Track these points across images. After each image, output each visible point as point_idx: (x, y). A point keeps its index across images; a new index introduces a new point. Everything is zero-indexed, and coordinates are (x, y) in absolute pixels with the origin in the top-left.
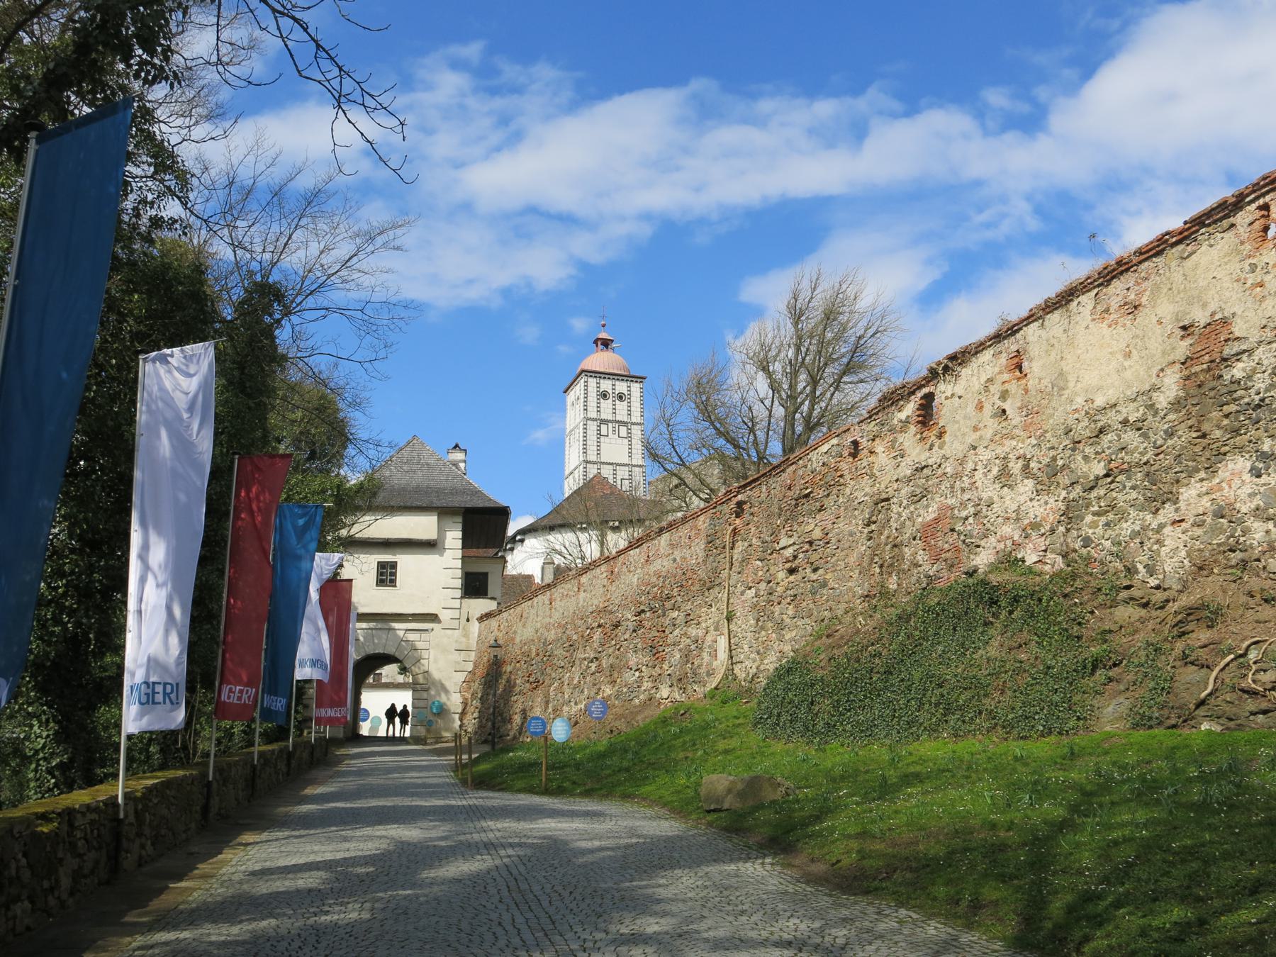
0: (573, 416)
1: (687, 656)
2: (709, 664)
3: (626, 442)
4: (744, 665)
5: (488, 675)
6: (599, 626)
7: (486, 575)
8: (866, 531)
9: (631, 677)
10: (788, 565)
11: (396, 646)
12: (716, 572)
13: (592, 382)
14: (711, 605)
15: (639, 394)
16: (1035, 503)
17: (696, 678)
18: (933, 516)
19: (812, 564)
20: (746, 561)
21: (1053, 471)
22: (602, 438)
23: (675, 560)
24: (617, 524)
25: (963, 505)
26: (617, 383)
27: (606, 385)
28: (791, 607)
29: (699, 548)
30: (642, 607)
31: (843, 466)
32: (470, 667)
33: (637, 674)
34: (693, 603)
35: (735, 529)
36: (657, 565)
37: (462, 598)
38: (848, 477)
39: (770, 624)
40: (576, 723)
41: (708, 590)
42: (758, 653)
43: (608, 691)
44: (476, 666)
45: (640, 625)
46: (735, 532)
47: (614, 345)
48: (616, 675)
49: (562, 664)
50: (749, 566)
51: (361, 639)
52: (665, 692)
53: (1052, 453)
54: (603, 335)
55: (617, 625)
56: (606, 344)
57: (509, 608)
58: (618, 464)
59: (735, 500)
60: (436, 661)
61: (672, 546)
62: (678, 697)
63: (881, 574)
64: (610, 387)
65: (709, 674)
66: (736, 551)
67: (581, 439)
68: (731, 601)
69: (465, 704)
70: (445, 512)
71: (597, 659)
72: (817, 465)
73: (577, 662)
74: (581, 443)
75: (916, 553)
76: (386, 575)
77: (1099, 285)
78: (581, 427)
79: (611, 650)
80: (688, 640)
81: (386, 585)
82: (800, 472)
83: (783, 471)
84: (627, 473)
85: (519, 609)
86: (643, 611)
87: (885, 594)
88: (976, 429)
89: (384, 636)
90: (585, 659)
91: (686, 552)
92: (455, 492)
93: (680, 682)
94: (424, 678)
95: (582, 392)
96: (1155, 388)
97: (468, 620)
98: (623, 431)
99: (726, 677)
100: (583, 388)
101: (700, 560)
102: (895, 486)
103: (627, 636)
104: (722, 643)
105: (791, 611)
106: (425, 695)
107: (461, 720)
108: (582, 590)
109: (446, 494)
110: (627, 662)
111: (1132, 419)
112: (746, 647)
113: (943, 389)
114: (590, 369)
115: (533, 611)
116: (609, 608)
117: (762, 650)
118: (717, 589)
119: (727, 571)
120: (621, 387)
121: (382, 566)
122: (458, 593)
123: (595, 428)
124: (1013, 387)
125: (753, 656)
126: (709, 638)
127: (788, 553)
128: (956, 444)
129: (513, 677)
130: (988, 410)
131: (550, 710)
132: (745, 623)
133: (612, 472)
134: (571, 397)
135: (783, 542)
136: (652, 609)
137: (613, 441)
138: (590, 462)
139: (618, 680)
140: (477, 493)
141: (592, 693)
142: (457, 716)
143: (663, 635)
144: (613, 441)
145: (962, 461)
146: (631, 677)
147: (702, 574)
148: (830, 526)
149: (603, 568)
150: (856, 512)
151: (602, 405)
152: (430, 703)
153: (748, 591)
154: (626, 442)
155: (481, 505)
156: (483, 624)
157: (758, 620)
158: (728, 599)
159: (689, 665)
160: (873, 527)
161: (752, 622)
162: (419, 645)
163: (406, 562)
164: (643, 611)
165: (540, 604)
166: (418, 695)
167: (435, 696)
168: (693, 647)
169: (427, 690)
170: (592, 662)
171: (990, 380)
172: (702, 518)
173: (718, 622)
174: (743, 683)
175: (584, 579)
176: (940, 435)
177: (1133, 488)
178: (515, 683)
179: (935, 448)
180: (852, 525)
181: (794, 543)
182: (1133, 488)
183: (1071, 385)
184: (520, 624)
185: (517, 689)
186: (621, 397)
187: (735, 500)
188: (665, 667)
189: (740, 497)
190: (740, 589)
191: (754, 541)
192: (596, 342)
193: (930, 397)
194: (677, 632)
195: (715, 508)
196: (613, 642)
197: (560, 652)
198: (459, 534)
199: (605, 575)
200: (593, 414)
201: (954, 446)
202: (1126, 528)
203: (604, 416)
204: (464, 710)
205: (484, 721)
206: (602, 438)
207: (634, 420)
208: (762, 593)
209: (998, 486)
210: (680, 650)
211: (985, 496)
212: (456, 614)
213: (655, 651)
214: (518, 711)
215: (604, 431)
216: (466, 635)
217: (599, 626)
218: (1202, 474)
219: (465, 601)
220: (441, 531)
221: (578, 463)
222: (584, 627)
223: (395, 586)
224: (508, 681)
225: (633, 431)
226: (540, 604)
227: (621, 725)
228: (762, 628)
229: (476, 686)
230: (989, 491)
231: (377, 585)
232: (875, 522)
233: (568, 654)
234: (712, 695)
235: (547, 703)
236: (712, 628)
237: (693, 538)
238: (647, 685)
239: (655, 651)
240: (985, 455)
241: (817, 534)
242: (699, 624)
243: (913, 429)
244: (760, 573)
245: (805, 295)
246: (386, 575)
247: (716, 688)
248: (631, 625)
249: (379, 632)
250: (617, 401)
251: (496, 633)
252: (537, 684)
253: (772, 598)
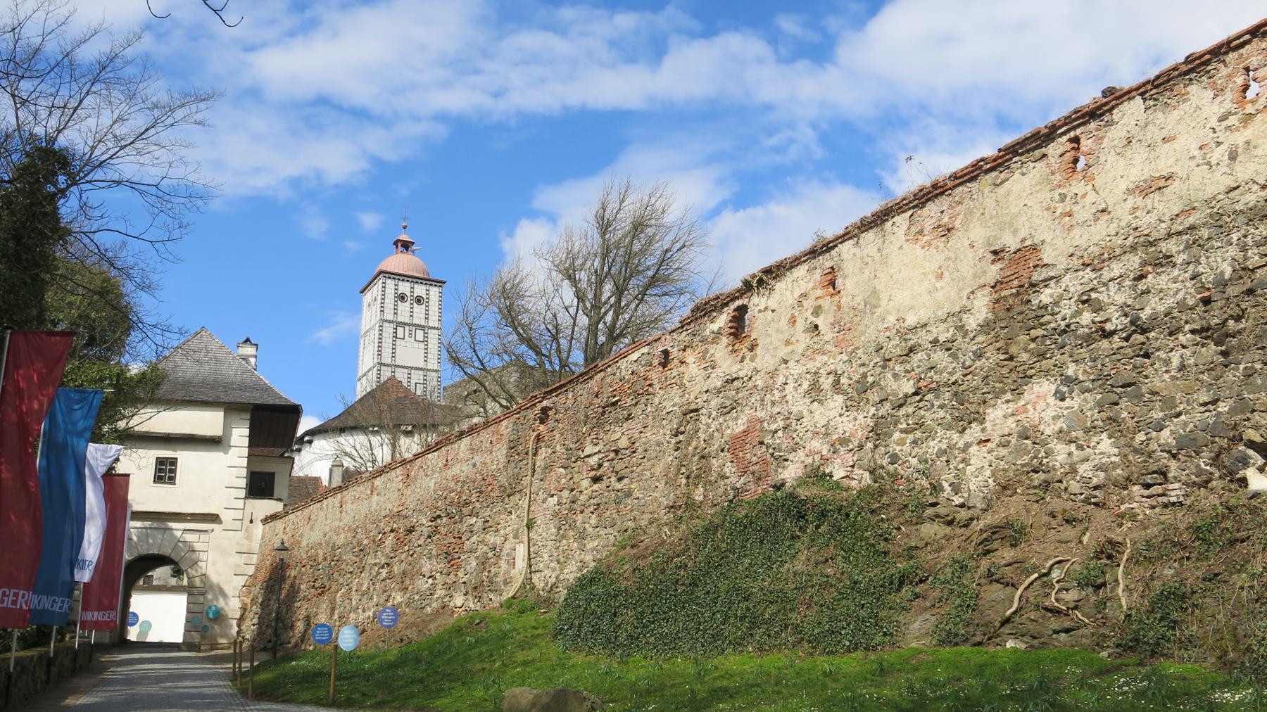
0: (369, 317)
1: (483, 564)
2: (507, 572)
3: (422, 346)
4: (543, 574)
5: (270, 579)
6: (392, 531)
7: (272, 475)
8: (673, 441)
9: (423, 584)
10: (592, 474)
11: (172, 547)
12: (518, 478)
13: (390, 284)
14: (511, 512)
15: (437, 299)
16: (844, 419)
17: (493, 587)
18: (742, 428)
19: (617, 473)
20: (548, 468)
21: (863, 387)
22: (398, 341)
23: (474, 465)
24: (410, 428)
25: (773, 418)
26: (416, 286)
27: (405, 287)
28: (594, 516)
29: (501, 453)
30: (438, 513)
31: (653, 375)
32: (251, 570)
33: (430, 581)
34: (492, 509)
35: (539, 435)
36: (455, 470)
37: (246, 498)
38: (657, 386)
39: (571, 533)
40: (363, 631)
41: (509, 496)
42: (558, 562)
43: (398, 598)
44: (257, 570)
45: (435, 531)
46: (539, 438)
47: (414, 248)
48: (407, 582)
49: (351, 570)
50: (552, 473)
51: (135, 538)
52: (459, 600)
53: (863, 370)
54: (404, 237)
55: (410, 531)
56: (406, 246)
57: (296, 510)
58: (412, 368)
59: (539, 406)
60: (214, 564)
61: (473, 450)
62: (472, 606)
63: (687, 485)
64: (409, 289)
65: (506, 583)
66: (539, 458)
67: (377, 341)
68: (532, 508)
69: (244, 609)
70: (232, 408)
71: (388, 565)
72: (626, 374)
73: (367, 568)
74: (376, 345)
75: (724, 465)
76: (165, 472)
77: (914, 207)
78: (377, 329)
79: (403, 556)
80: (486, 548)
81: (165, 483)
82: (608, 380)
83: (591, 378)
84: (422, 378)
85: (307, 511)
86: (439, 516)
87: (691, 505)
88: (788, 343)
89: (160, 536)
90: (375, 564)
91: (488, 459)
92: (244, 387)
93: (476, 590)
94: (202, 581)
95: (380, 293)
96: (965, 310)
97: (251, 522)
98: (420, 334)
99: (523, 585)
100: (380, 286)
101: (501, 466)
102: (705, 397)
103: (421, 542)
104: (521, 551)
105: (594, 521)
106: (201, 599)
107: (239, 626)
108: (375, 493)
109: (234, 389)
110: (420, 568)
111: (941, 339)
112: (546, 556)
113: (756, 302)
114: (389, 270)
115: (322, 514)
116: (403, 513)
117: (562, 560)
118: (518, 496)
119: (528, 478)
120: (420, 290)
121: (161, 462)
122: (242, 493)
124: (826, 303)
125: (553, 565)
126: (508, 546)
127: (593, 461)
128: (768, 357)
129: (297, 582)
130: (801, 325)
131: (336, 617)
132: (545, 531)
133: (406, 376)
134: (368, 297)
135: (589, 449)
136: (448, 514)
137: (408, 344)
138: (384, 365)
139: (410, 587)
140: (267, 389)
141: (382, 601)
142: (234, 622)
143: (459, 542)
144: (408, 344)
145: (773, 375)
146: (423, 584)
147: (503, 480)
148: (637, 435)
149: (399, 471)
150: (664, 422)
151: (399, 308)
152: (206, 607)
153: (549, 499)
154: (422, 346)
155: (271, 402)
156: (267, 526)
157: (559, 529)
158: (529, 507)
159: (487, 574)
160: (681, 437)
161: (554, 530)
162: (197, 546)
163: (187, 459)
164: (439, 516)
165: (330, 507)
166: (193, 599)
167: (212, 601)
168: (490, 555)
169: (203, 594)
170: (383, 567)
171: (804, 295)
172: (505, 423)
173: (518, 530)
174: (541, 593)
175: (378, 482)
176: (752, 348)
177: (941, 407)
178: (299, 588)
179: (747, 361)
180: (660, 434)
181: (600, 452)
182: (941, 407)
183: (883, 303)
184: (308, 527)
185: (301, 595)
186: (419, 300)
187: (539, 406)
188: (461, 574)
189: (545, 403)
190: (541, 496)
191: (558, 447)
192: (396, 243)
193: (743, 310)
194: (474, 539)
195: (518, 413)
196: (407, 548)
197: (349, 557)
198: (246, 432)
199: (400, 478)
200: (390, 317)
201: (765, 359)
202: (933, 446)
203: (400, 319)
204: (242, 615)
205: (264, 628)
206: (398, 341)
207: (431, 324)
208: (564, 501)
209: (808, 401)
210: (477, 558)
211: (795, 409)
212: (239, 515)
213: (450, 558)
214: (301, 617)
215: (400, 334)
216: (249, 538)
217: (392, 531)
218: (1008, 396)
219: (247, 501)
220: (227, 427)
221: (372, 365)
222: (377, 532)
223: (174, 484)
224: (292, 586)
225: (430, 336)
226: (330, 507)
227: (412, 634)
228: (563, 537)
229: (257, 590)
230: (799, 405)
231: (154, 482)
232: (682, 433)
233: (357, 559)
234: (509, 604)
235: (333, 609)
236: (511, 536)
237: (494, 443)
238: (440, 593)
239: (450, 558)
240: (796, 369)
241: (623, 443)
242: (497, 531)
243: (725, 340)
244: (564, 481)
245: (613, 205)
246: (165, 472)
247: (513, 597)
248: (426, 531)
249: (155, 532)
250: (415, 304)
251: (281, 535)
252: (323, 590)
253: (575, 506)
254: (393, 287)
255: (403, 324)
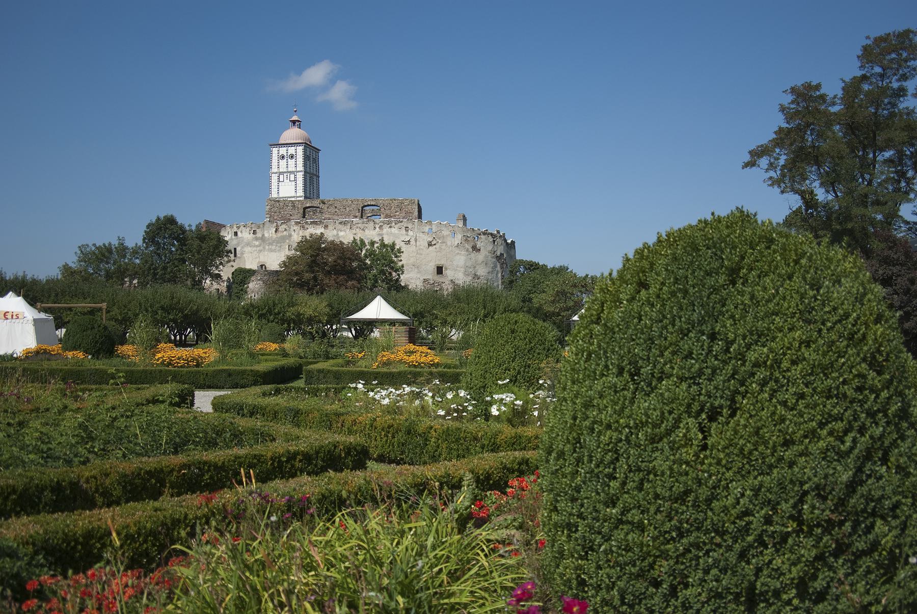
13: (275, 150)
27: (283, 151)
54: (295, 118)
98: (292, 177)
120: (291, 150)
123: (277, 178)
186: (292, 157)
203: (281, 170)
207: (298, 169)
215: (281, 179)
254: (277, 152)
255: (283, 173)
